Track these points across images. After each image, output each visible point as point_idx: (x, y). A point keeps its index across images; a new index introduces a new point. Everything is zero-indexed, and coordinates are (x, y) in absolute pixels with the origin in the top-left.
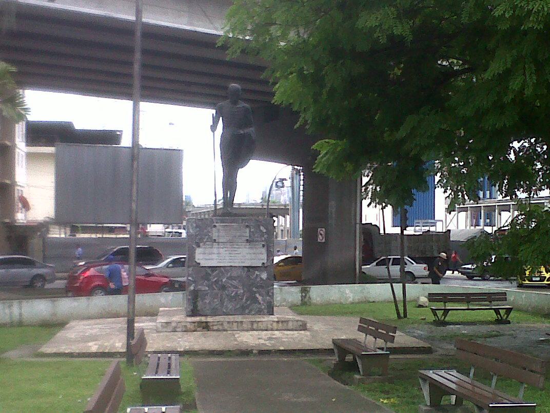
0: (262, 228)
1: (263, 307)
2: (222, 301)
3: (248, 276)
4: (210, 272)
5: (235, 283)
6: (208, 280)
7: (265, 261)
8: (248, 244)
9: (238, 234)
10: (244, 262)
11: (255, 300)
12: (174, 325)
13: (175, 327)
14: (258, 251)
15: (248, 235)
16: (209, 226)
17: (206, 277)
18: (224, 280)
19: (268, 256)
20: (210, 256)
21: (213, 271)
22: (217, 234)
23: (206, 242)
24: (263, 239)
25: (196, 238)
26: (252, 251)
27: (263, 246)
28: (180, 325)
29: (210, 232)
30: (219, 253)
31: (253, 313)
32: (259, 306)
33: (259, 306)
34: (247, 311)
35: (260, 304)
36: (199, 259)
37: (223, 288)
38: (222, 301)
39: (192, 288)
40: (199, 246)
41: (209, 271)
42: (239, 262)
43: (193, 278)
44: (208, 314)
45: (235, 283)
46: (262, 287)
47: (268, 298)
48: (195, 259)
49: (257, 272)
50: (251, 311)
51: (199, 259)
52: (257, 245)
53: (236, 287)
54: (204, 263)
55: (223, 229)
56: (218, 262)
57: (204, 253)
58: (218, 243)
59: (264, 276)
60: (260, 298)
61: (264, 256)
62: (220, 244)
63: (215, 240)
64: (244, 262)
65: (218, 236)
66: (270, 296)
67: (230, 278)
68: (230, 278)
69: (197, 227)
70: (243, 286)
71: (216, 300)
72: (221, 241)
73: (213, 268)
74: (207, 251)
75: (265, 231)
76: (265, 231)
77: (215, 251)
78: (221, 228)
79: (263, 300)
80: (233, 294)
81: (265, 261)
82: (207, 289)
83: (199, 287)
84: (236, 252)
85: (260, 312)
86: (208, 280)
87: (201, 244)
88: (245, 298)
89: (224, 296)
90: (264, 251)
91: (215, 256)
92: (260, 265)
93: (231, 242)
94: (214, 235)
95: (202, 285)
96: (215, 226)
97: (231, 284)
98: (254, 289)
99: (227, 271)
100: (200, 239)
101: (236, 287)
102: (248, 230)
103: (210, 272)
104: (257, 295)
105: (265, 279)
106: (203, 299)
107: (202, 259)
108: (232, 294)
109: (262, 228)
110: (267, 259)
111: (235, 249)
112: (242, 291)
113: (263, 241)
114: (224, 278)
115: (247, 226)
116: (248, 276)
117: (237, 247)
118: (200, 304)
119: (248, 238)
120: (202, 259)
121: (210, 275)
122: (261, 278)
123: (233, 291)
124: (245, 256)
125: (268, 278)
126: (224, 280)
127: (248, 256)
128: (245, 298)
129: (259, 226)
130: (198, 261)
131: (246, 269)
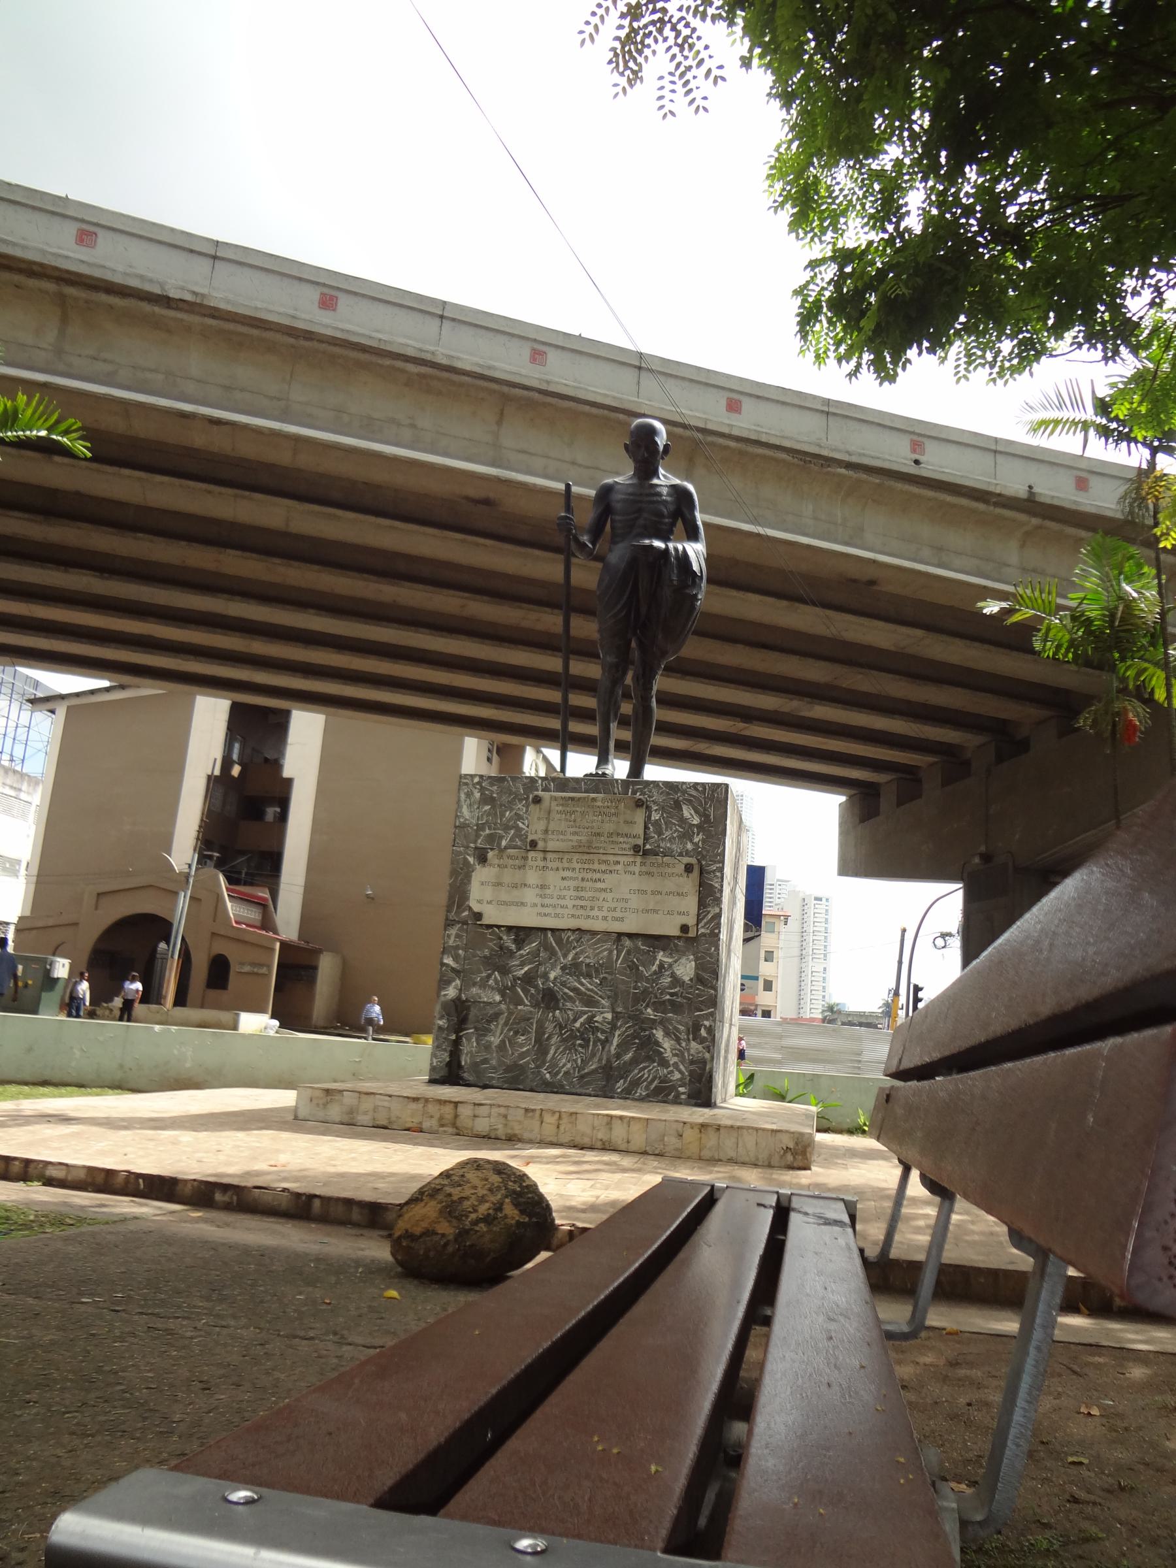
0: (687, 812)
1: (677, 1076)
2: (541, 1047)
3: (633, 968)
4: (513, 947)
5: (586, 985)
6: (504, 971)
7: (691, 921)
8: (639, 859)
9: (609, 827)
10: (622, 919)
11: (648, 1050)
12: (349, 1099)
13: (351, 1111)
14: (670, 885)
15: (641, 832)
16: (520, 800)
17: (498, 962)
18: (552, 975)
19: (702, 904)
20: (515, 895)
21: (520, 943)
22: (541, 825)
23: (506, 848)
24: (689, 846)
25: (478, 836)
26: (650, 884)
27: (689, 868)
28: (367, 1104)
29: (519, 817)
30: (543, 887)
31: (641, 1091)
32: (663, 1071)
33: (663, 1071)
34: (620, 1086)
35: (664, 1063)
36: (479, 902)
37: (549, 999)
38: (541, 1047)
39: (451, 992)
40: (483, 859)
41: (508, 941)
42: (605, 918)
43: (456, 958)
44: (494, 1082)
45: (586, 985)
46: (676, 1007)
47: (693, 1044)
48: (468, 898)
49: (660, 956)
50: (636, 1083)
51: (479, 902)
52: (668, 865)
53: (590, 1002)
54: (492, 915)
55: (560, 808)
56: (539, 914)
57: (499, 884)
58: (545, 851)
59: (686, 969)
60: (667, 1045)
61: (690, 904)
62: (549, 856)
63: (534, 844)
64: (622, 919)
65: (546, 831)
66: (702, 1041)
67: (574, 968)
68: (574, 968)
69: (486, 799)
70: (614, 999)
71: (521, 1039)
72: (551, 845)
73: (522, 934)
74: (508, 877)
75: (696, 821)
76: (696, 821)
77: (532, 877)
78: (556, 808)
79: (679, 1054)
80: (582, 1020)
81: (691, 921)
82: (498, 998)
83: (474, 990)
84: (599, 885)
85: (662, 1093)
86: (504, 971)
87: (490, 854)
88: (615, 1042)
89: (550, 1027)
90: (689, 885)
91: (530, 895)
92: (675, 932)
93: (585, 850)
94: (533, 828)
95: (483, 985)
96: (537, 800)
97: (575, 990)
98: (649, 1010)
99: (566, 947)
100: (491, 839)
101: (590, 1002)
102: (640, 816)
103: (513, 947)
104: (659, 1034)
105: (686, 979)
106: (482, 1032)
107: (489, 902)
108: (575, 1020)
109: (687, 812)
110: (698, 915)
111: (598, 876)
112: (609, 1016)
113: (688, 854)
114: (553, 967)
115: (639, 804)
116: (633, 968)
117: (603, 867)
118: (469, 1048)
119: (640, 842)
120: (489, 902)
121: (511, 954)
122: (673, 975)
123: (585, 1012)
124: (626, 901)
125: (699, 979)
126: (552, 975)
127: (635, 902)
128: (615, 1042)
129: (678, 805)
130: (476, 908)
131: (627, 943)
